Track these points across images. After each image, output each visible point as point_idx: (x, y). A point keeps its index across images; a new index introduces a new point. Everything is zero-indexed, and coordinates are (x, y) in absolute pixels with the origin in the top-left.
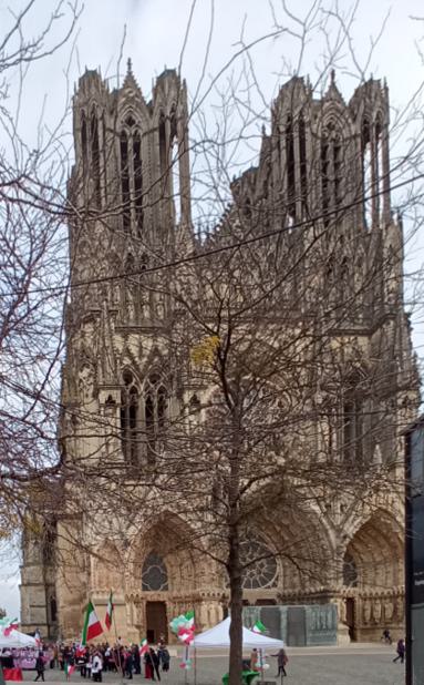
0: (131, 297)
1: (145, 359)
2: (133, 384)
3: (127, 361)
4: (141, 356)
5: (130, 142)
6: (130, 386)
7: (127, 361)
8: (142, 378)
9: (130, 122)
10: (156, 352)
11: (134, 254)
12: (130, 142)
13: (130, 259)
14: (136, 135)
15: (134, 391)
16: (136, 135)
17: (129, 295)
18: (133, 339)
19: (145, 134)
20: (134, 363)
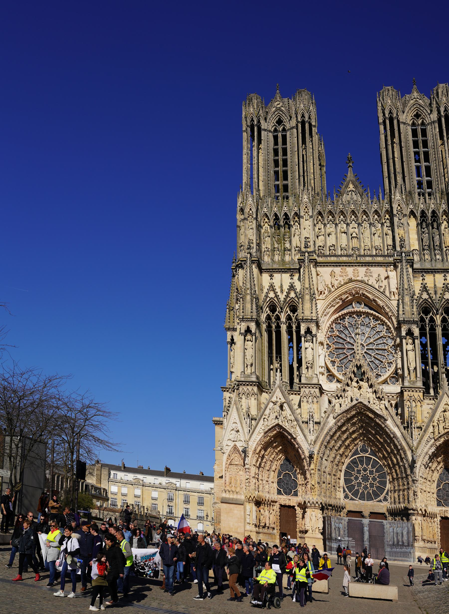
0: (276, 246)
1: (285, 293)
2: (277, 312)
3: (272, 295)
4: (282, 291)
5: (280, 135)
7: (272, 295)
10: (292, 287)
12: (280, 135)
13: (277, 218)
14: (284, 130)
15: (278, 318)
16: (284, 130)
17: (275, 243)
20: (277, 296)
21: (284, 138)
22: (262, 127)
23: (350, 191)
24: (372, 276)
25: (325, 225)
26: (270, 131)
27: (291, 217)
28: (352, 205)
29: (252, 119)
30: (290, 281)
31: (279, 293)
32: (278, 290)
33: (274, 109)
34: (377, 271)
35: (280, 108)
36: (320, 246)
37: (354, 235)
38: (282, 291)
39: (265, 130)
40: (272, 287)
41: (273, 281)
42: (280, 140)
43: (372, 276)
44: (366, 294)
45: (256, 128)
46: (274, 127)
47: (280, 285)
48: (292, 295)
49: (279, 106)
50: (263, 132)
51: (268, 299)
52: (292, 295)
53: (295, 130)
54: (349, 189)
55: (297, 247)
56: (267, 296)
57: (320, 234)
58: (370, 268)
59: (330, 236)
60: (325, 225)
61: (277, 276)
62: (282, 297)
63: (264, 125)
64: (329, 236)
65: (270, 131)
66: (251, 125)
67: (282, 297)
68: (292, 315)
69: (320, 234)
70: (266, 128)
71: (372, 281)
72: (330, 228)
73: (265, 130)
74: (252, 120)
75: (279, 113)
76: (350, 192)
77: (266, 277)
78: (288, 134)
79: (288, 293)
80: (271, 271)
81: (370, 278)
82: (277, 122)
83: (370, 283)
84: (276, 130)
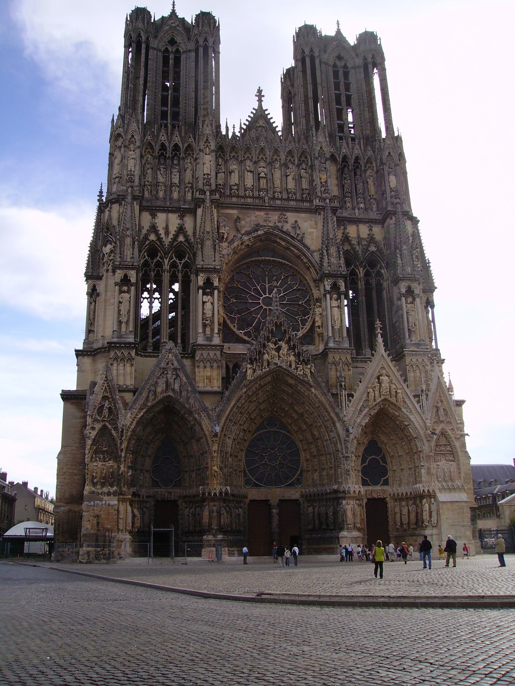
1: (171, 236)
2: (158, 258)
3: (152, 237)
4: (167, 233)
5: (172, 56)
6: (155, 261)
7: (152, 237)
8: (166, 253)
9: (172, 42)
10: (181, 230)
11: (167, 145)
12: (172, 56)
15: (159, 265)
16: (177, 51)
18: (161, 218)
19: (184, 52)
20: (159, 239)
21: (177, 60)
22: (151, 45)
23: (260, 126)
24: (287, 222)
25: (226, 162)
26: (160, 51)
27: (182, 150)
28: (262, 142)
29: (140, 34)
30: (179, 221)
31: (163, 236)
32: (162, 232)
33: (168, 27)
34: (291, 217)
35: (175, 27)
36: (220, 185)
37: (262, 175)
38: (167, 233)
39: (154, 49)
40: (154, 229)
41: (156, 221)
42: (171, 62)
43: (287, 222)
44: (278, 240)
45: (144, 46)
46: (165, 47)
47: (164, 226)
48: (181, 238)
49: (173, 25)
50: (151, 52)
51: (147, 242)
52: (181, 238)
53: (194, 54)
54: (258, 125)
55: (189, 183)
56: (146, 238)
57: (220, 171)
58: (285, 213)
59: (233, 174)
60: (226, 162)
61: (161, 217)
62: (167, 241)
63: (154, 43)
64: (231, 173)
65: (160, 51)
66: (137, 41)
67: (167, 241)
68: (178, 261)
69: (220, 171)
70: (156, 47)
71: (287, 227)
72: (234, 166)
73: (154, 49)
74: (139, 36)
75: (173, 33)
76: (260, 128)
77: (146, 217)
78: (183, 57)
79: (176, 236)
80: (153, 211)
81: (285, 224)
82: (169, 42)
83: (285, 229)
84: (166, 50)
